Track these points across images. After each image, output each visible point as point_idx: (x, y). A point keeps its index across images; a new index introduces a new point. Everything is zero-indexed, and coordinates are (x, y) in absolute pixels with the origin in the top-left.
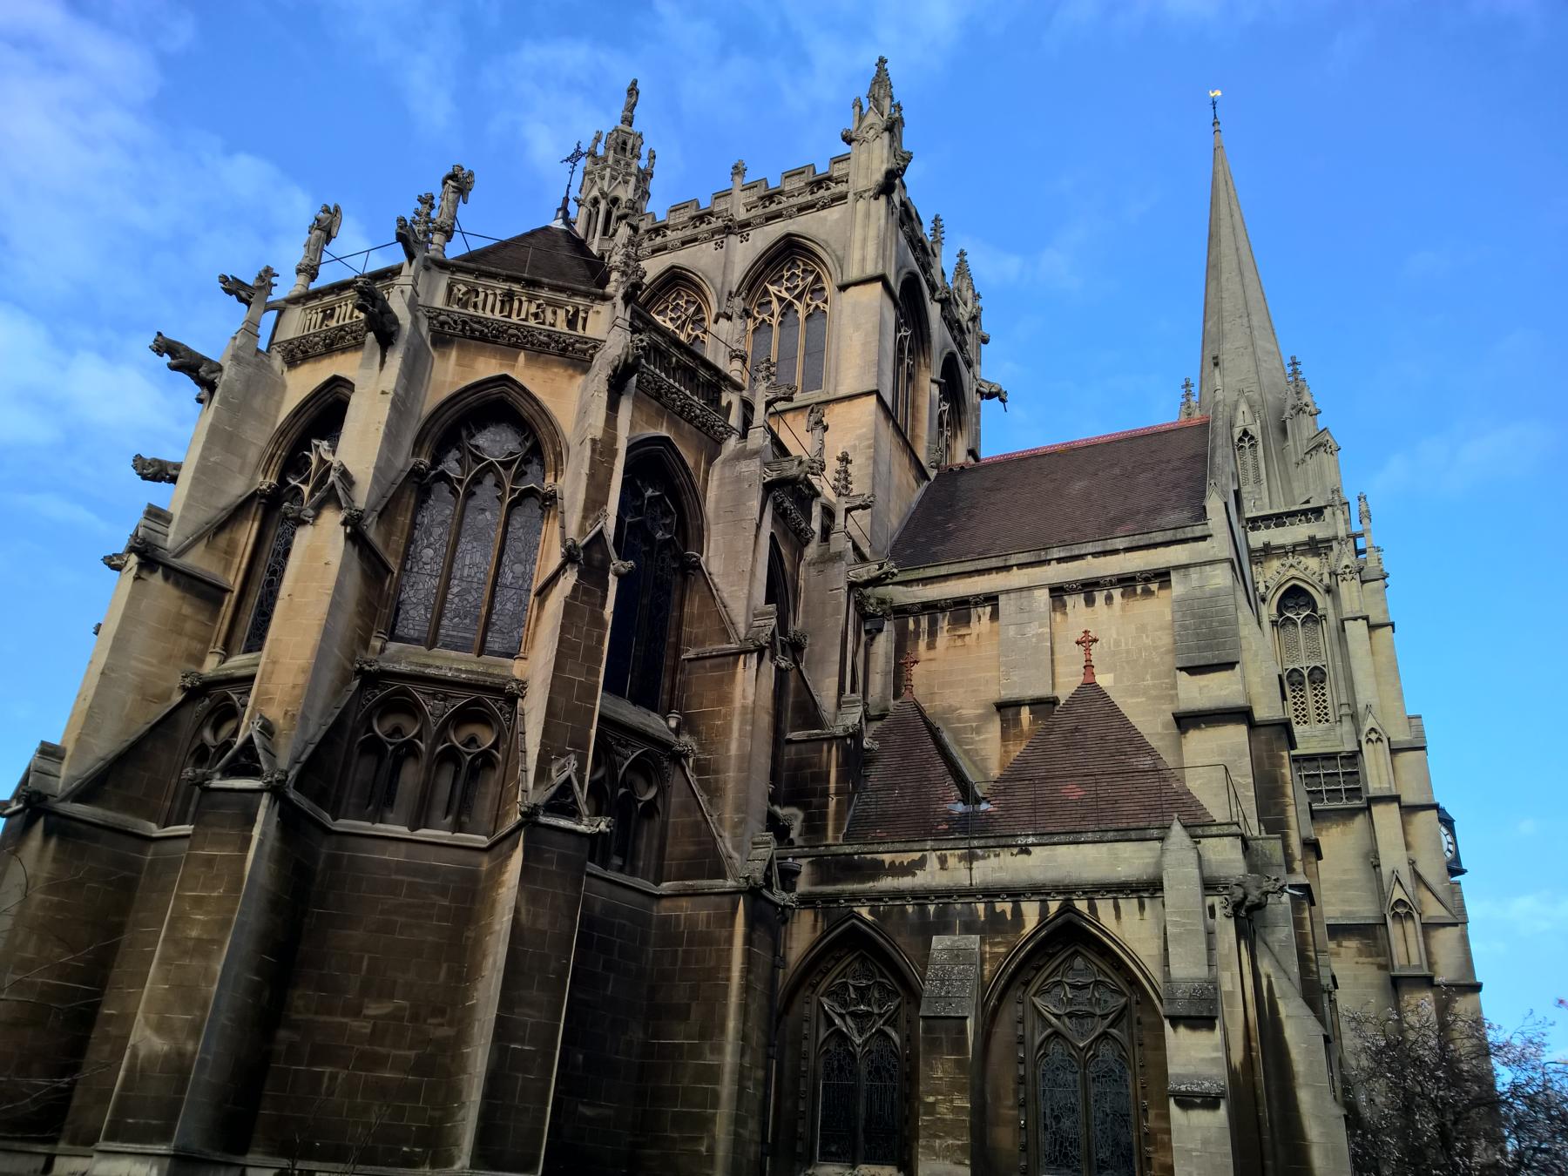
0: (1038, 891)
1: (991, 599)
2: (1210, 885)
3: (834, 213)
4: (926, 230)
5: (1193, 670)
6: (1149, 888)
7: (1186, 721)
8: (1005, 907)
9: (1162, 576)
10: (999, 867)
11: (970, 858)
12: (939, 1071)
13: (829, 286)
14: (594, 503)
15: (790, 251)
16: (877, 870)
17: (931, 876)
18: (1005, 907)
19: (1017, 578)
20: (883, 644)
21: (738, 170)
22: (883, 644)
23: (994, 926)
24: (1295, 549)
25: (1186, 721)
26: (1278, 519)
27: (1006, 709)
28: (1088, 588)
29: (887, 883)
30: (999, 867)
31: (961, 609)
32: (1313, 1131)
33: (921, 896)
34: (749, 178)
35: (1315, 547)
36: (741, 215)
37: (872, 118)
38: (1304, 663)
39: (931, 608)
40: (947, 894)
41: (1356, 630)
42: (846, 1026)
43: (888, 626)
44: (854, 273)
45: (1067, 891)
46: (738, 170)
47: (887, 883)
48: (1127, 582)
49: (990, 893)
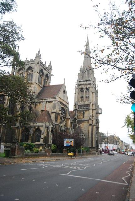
0: (37, 126)
1: (42, 102)
2: (46, 126)
3: (34, 65)
4: (44, 63)
5: (53, 109)
6: (42, 126)
7: (52, 113)
8: (35, 127)
9: (53, 101)
10: (35, 124)
11: (34, 124)
12: (30, 137)
13: (33, 72)
14: (7, 104)
15: (30, 68)
16: (28, 124)
17: (31, 125)
18: (35, 127)
19: (43, 100)
20: (34, 105)
21: (27, 59)
22: (34, 105)
23: (35, 128)
24: (88, 84)
25: (52, 113)
26: (87, 81)
27: (42, 111)
28: (48, 102)
29: (29, 125)
30: (35, 124)
31: (40, 103)
32: (49, 139)
33: (31, 126)
34: (28, 60)
35: (90, 84)
36: (27, 63)
37: (38, 55)
38: (87, 96)
39: (38, 102)
40: (32, 126)
41: (91, 93)
42: (26, 134)
43: (35, 104)
44: (35, 71)
45: (39, 126)
46: (27, 59)
47: (29, 125)
48: (51, 101)
49: (34, 126)
